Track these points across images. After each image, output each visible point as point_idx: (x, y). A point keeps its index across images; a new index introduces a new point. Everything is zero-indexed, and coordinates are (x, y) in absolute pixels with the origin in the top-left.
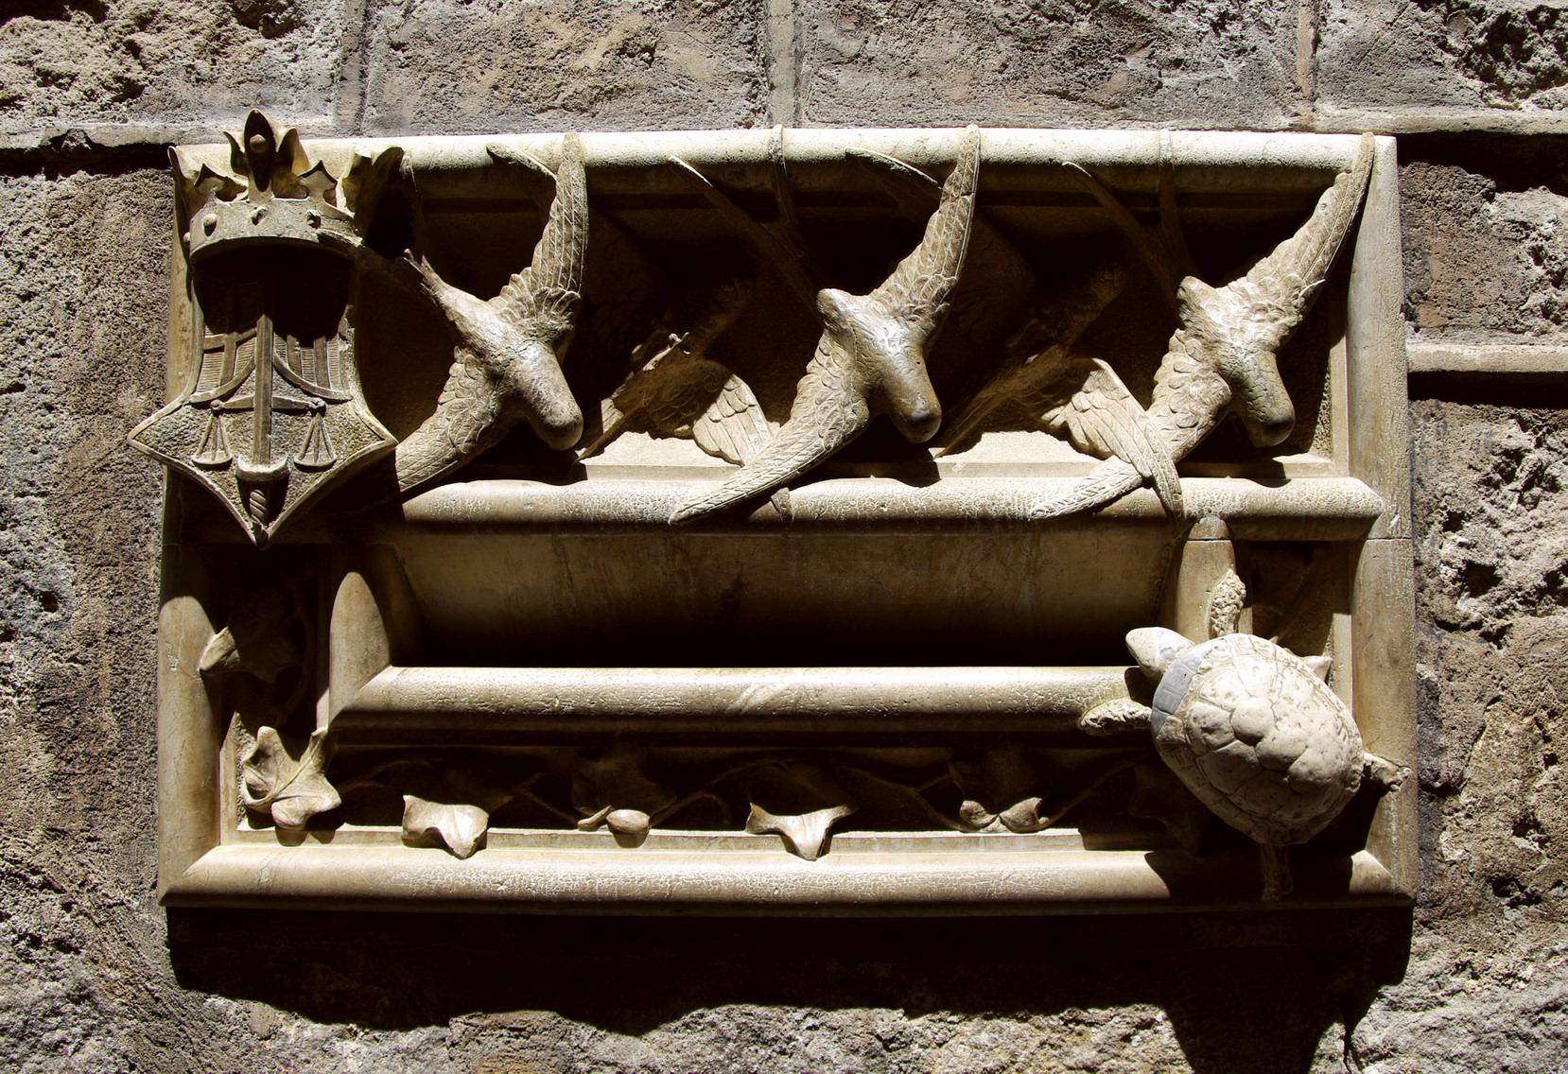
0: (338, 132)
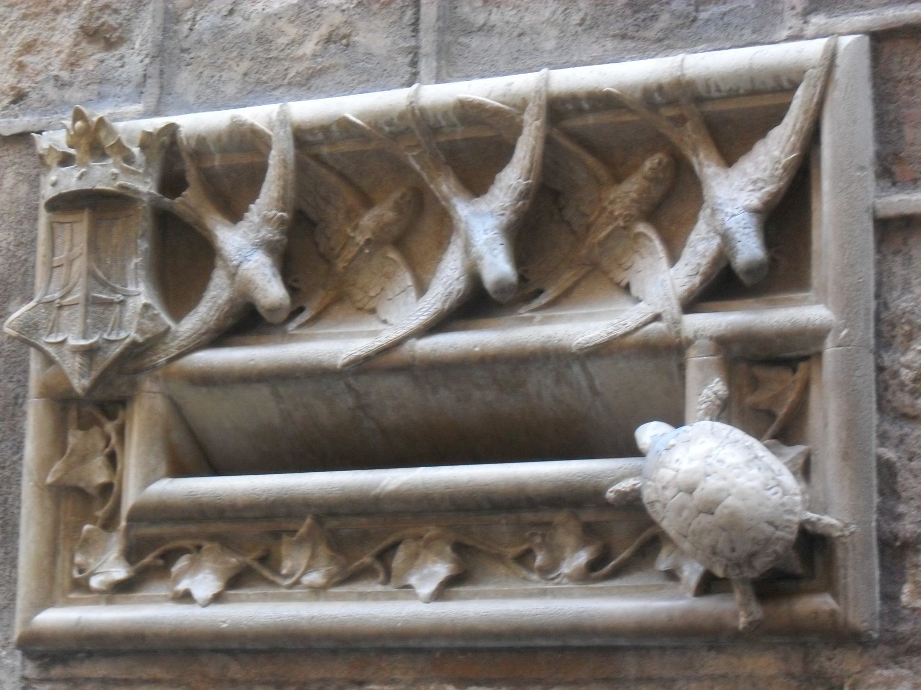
0: (146, 115)
